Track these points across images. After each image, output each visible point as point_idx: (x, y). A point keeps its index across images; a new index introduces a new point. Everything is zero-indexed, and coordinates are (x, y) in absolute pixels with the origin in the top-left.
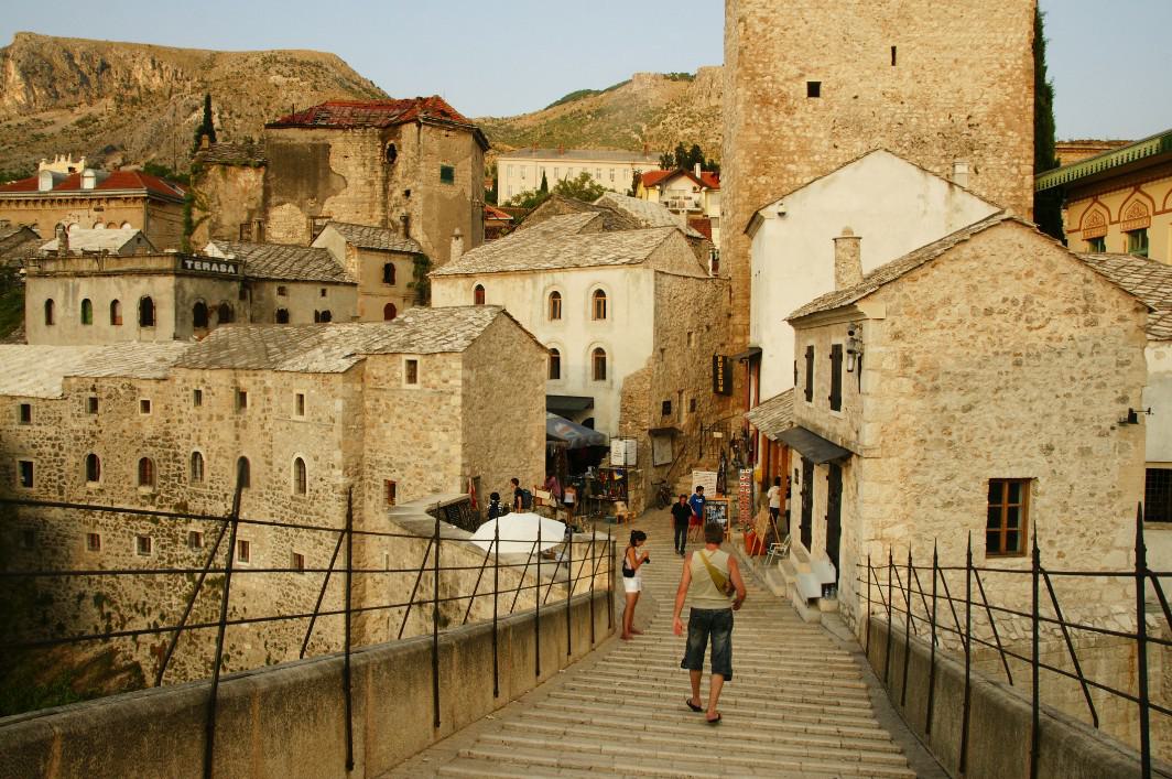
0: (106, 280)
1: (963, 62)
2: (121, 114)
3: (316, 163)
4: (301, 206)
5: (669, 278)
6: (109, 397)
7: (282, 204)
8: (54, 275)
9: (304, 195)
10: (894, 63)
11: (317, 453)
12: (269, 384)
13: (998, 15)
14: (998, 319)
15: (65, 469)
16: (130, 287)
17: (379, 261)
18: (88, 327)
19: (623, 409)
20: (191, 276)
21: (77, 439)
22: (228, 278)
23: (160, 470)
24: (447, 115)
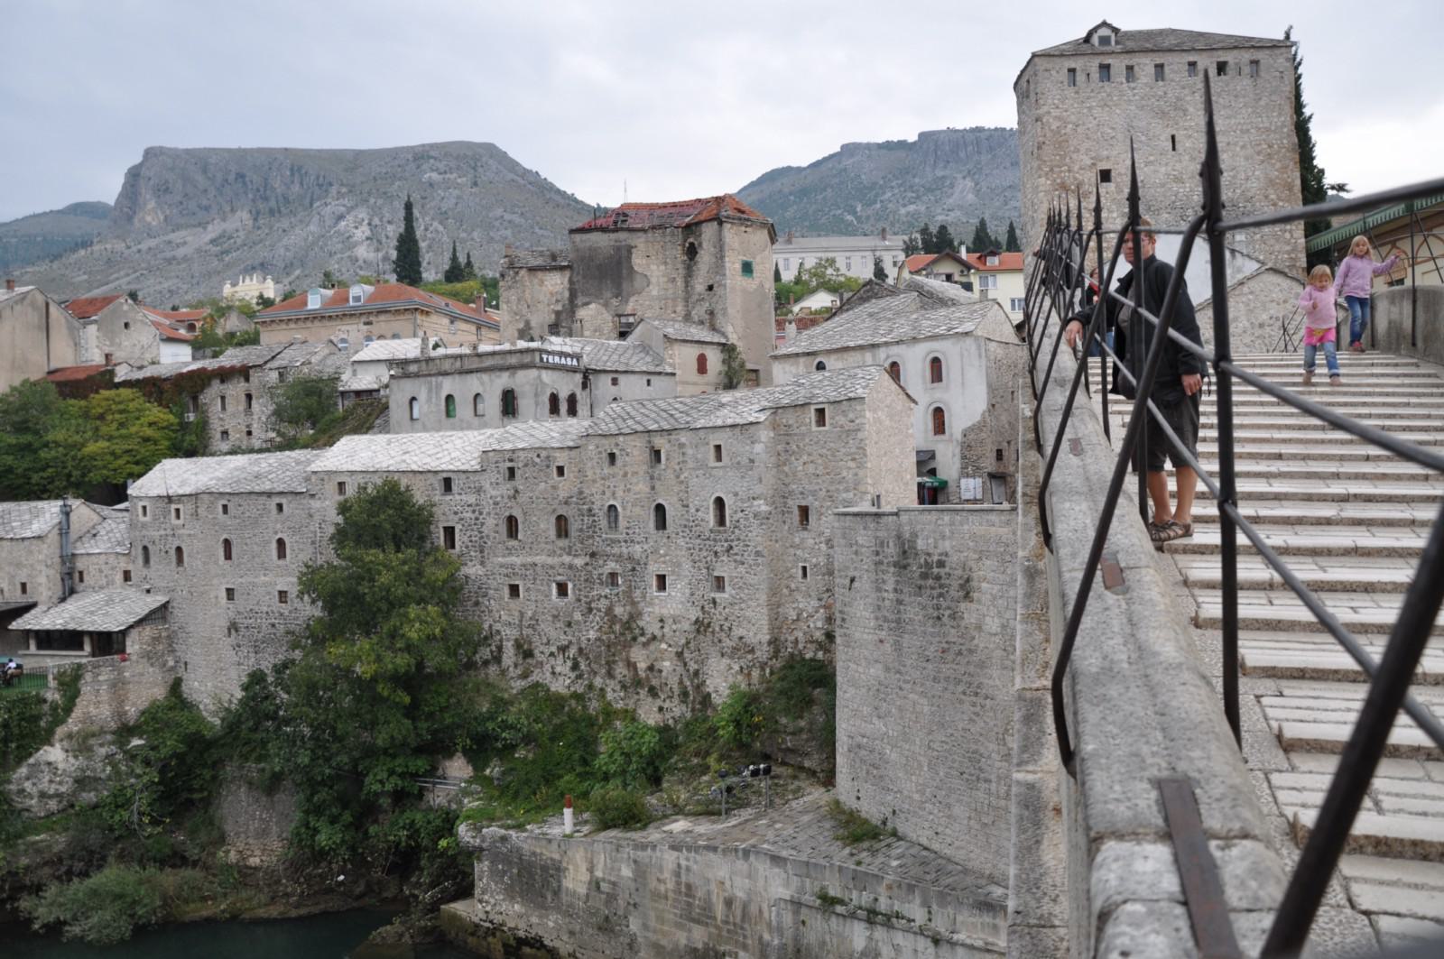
0: (469, 377)
1: (1236, 144)
2: (259, 228)
3: (619, 263)
4: (606, 305)
5: (994, 344)
6: (526, 465)
7: (587, 304)
8: (417, 375)
9: (609, 295)
10: (1174, 149)
11: (737, 489)
12: (683, 440)
13: (1262, 103)
14: (1268, 329)
15: (485, 529)
16: (491, 381)
17: (693, 352)
18: (451, 420)
19: (964, 457)
20: (546, 368)
21: (496, 504)
22: (574, 370)
23: (574, 527)
24: (743, 212)
